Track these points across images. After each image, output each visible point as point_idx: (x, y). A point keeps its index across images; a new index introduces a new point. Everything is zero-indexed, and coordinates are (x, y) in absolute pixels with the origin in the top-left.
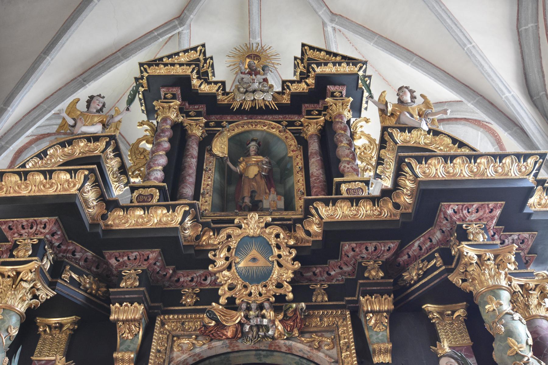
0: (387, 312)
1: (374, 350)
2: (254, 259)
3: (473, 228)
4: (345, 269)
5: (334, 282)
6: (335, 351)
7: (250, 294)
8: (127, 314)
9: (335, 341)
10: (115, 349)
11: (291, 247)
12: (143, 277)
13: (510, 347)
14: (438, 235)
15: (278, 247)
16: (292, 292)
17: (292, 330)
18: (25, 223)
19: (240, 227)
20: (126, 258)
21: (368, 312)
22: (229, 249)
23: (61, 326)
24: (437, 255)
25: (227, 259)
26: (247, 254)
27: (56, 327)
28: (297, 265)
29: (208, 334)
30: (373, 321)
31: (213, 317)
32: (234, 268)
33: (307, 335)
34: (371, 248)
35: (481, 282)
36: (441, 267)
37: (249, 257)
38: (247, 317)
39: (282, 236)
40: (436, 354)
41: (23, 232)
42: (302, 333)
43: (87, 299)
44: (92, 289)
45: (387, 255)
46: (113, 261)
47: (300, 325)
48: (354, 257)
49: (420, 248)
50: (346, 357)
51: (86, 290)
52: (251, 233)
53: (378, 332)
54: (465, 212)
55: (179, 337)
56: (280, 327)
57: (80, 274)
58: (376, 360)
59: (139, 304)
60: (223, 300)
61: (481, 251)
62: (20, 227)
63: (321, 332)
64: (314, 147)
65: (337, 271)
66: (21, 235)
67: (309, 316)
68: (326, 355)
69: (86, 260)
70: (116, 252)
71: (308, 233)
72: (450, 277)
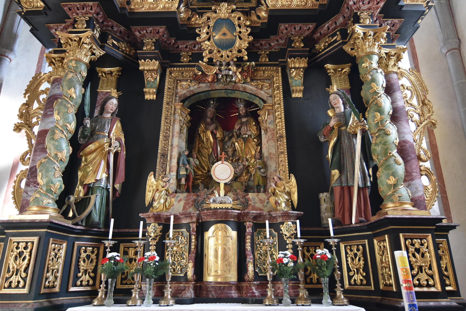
0: (303, 68)
1: (293, 90)
2: (224, 34)
3: (364, 15)
4: (281, 42)
5: (273, 50)
6: (270, 90)
7: (222, 56)
8: (149, 66)
9: (271, 85)
10: (144, 87)
11: (248, 26)
12: (157, 44)
13: (372, 88)
14: (341, 20)
15: (240, 26)
16: (247, 55)
17: (246, 78)
18: (78, 6)
19: (216, 12)
20: (145, 32)
21: (292, 68)
22: (209, 27)
23: (111, 73)
24: (338, 33)
25: (207, 33)
26: (220, 31)
27: (108, 74)
28: (251, 38)
29: (197, 79)
30: (294, 74)
31: (200, 69)
32: (212, 39)
33: (255, 81)
34: (298, 28)
35: (363, 50)
36: (339, 40)
37: (221, 33)
38: (220, 70)
39: (242, 19)
40: (328, 92)
41: (78, 12)
42: (252, 80)
43: (124, 57)
44: (127, 51)
45: (307, 33)
46: (137, 33)
47: (251, 75)
48: (286, 33)
49: (328, 28)
50: (277, 94)
51: (123, 51)
52: (222, 16)
53: (297, 80)
54: (361, 3)
55: (180, 81)
56: (239, 76)
57: (118, 41)
58: (294, 95)
59: (156, 60)
60: (205, 60)
61: (366, 30)
62: (76, 8)
63: (263, 80)
65: (275, 43)
66: (78, 14)
67: (256, 70)
68: (265, 93)
69: (120, 32)
70: (139, 28)
71: (259, 17)
72: (344, 47)
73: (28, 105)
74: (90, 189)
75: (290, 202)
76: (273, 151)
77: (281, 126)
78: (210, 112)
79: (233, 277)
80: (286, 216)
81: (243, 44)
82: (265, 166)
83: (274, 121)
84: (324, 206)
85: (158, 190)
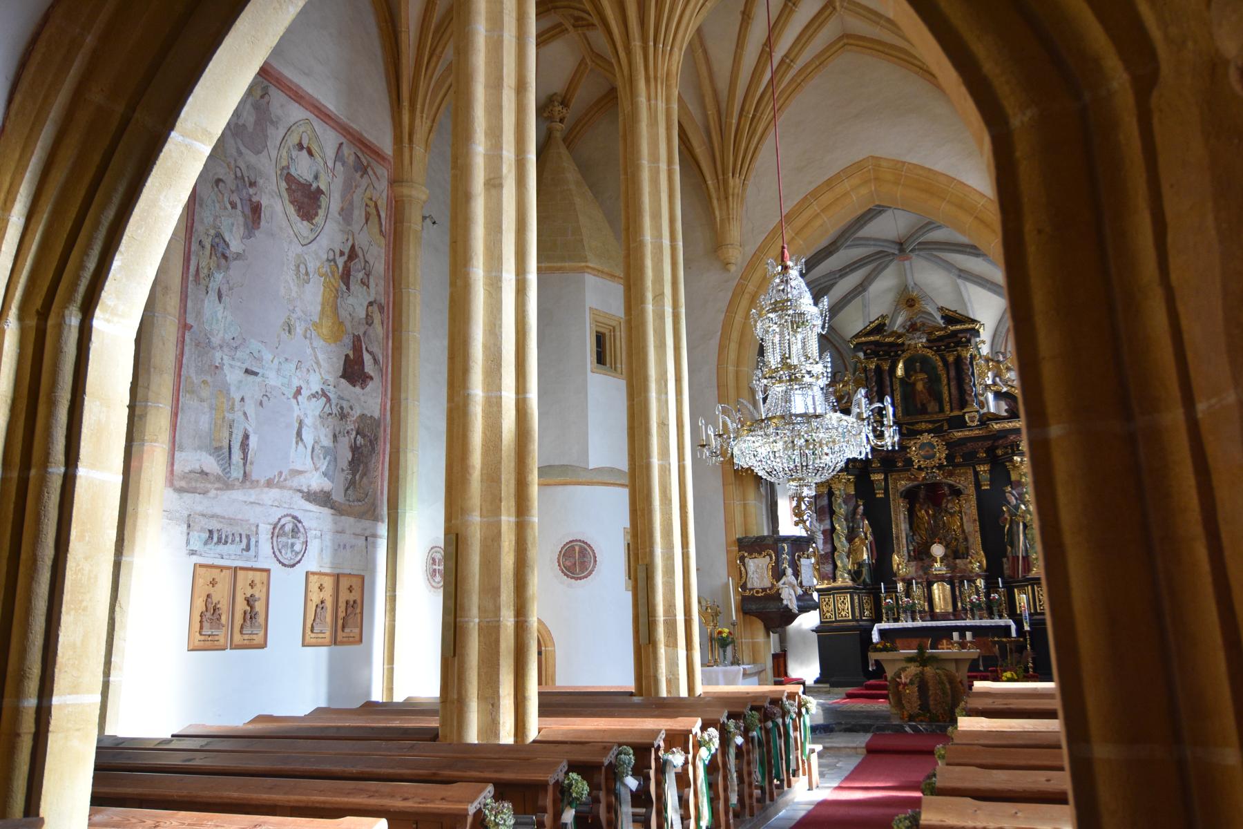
47: (951, 474)
64: (953, 373)
73: (798, 506)
74: (860, 565)
75: (980, 567)
76: (971, 529)
77: (974, 511)
78: (922, 494)
79: (950, 609)
80: (979, 576)
81: (941, 454)
82: (966, 539)
83: (970, 507)
84: (1005, 566)
85: (898, 561)
